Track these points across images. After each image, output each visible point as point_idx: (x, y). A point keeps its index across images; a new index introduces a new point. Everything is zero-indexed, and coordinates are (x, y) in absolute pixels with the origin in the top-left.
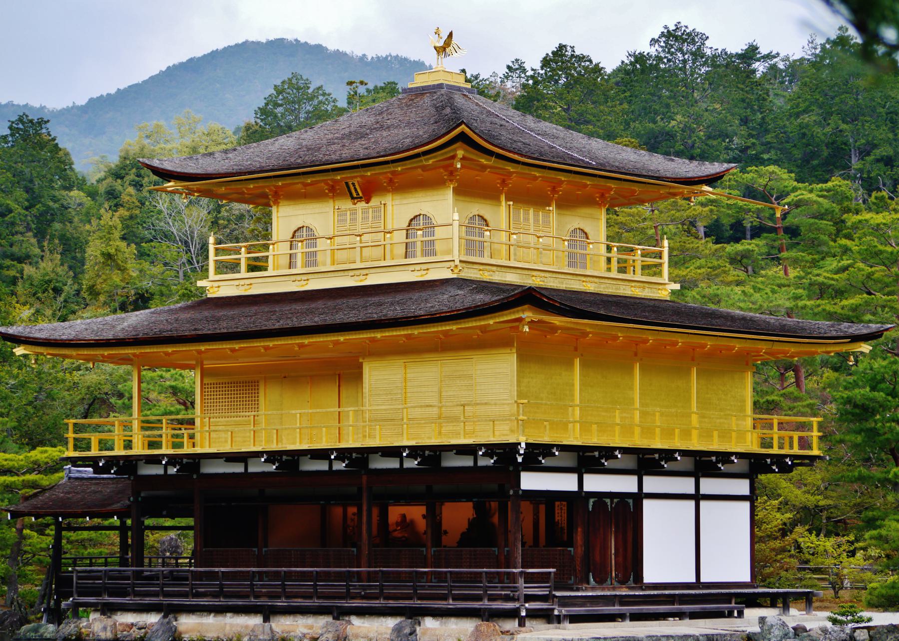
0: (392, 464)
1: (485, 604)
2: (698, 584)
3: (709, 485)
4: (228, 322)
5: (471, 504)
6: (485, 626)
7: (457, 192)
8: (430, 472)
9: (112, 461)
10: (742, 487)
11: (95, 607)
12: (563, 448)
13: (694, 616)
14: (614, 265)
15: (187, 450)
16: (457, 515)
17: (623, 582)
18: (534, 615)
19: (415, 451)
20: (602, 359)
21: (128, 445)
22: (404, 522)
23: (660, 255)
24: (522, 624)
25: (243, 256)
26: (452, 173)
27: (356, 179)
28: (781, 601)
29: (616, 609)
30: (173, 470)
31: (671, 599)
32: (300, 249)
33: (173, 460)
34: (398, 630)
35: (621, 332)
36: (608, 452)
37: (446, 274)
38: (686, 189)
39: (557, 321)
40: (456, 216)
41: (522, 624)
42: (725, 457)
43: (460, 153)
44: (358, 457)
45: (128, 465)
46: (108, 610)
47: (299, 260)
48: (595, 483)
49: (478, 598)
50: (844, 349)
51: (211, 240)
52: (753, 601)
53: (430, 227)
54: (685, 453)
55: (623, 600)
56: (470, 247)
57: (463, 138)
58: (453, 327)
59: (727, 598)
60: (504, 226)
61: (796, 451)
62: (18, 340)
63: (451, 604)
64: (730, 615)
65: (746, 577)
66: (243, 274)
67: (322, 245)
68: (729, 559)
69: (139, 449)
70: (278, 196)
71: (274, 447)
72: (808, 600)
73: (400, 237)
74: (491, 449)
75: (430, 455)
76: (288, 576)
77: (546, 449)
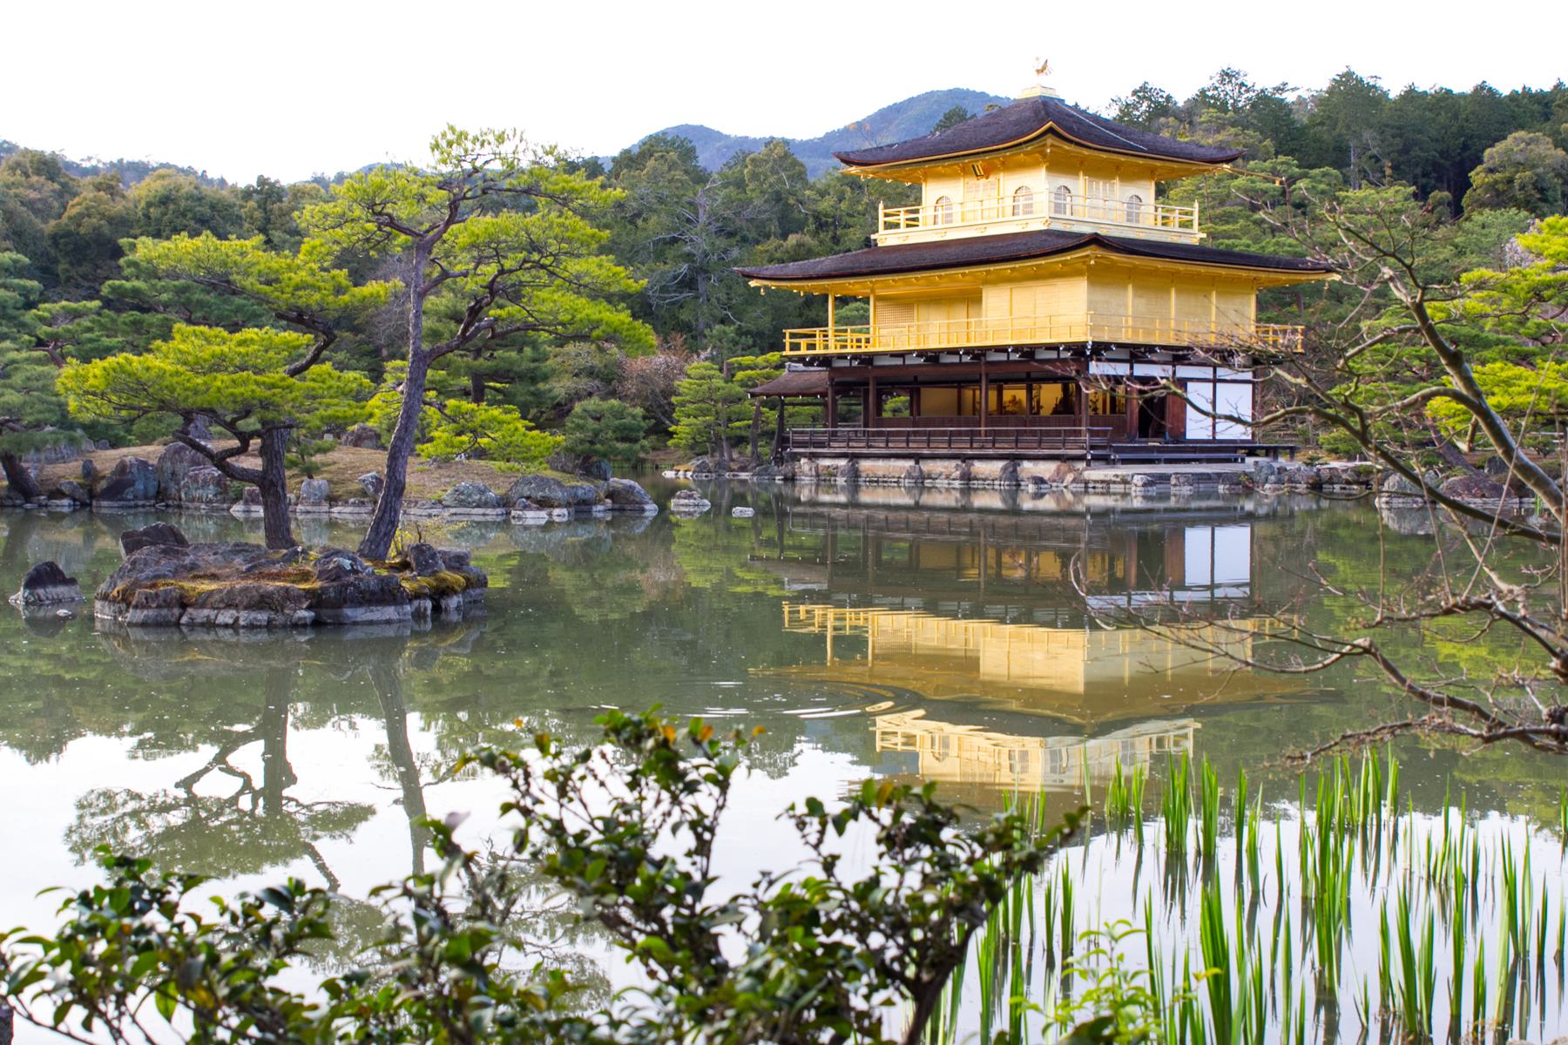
0: (1002, 357)
2: (1214, 440)
3: (1222, 372)
4: (891, 261)
5: (1059, 386)
6: (1064, 467)
7: (1049, 169)
8: (1027, 364)
9: (814, 358)
11: (803, 455)
12: (1119, 345)
13: (1209, 461)
14: (1160, 221)
15: (863, 350)
16: (1050, 395)
18: (1096, 458)
19: (1017, 348)
20: (1148, 284)
21: (826, 347)
22: (1014, 401)
23: (1191, 214)
24: (1088, 465)
26: (1044, 155)
27: (979, 165)
28: (1272, 452)
29: (1155, 455)
30: (855, 363)
31: (1195, 450)
32: (939, 213)
33: (855, 356)
34: (1004, 469)
35: (1159, 264)
36: (1151, 348)
37: (1037, 226)
38: (1210, 167)
39: (1115, 257)
44: (978, 353)
45: (825, 361)
46: (813, 457)
47: (939, 220)
48: (1141, 370)
50: (1320, 277)
51: (881, 206)
52: (1252, 452)
53: (1029, 196)
55: (1159, 450)
56: (1059, 208)
58: (1042, 262)
59: (1235, 450)
60: (1081, 192)
62: (752, 277)
64: (1236, 460)
66: (903, 228)
67: (956, 210)
69: (832, 351)
70: (926, 176)
71: (922, 347)
72: (1292, 451)
73: (1009, 202)
74: (1069, 347)
75: (1028, 352)
76: (930, 434)
77: (1106, 346)
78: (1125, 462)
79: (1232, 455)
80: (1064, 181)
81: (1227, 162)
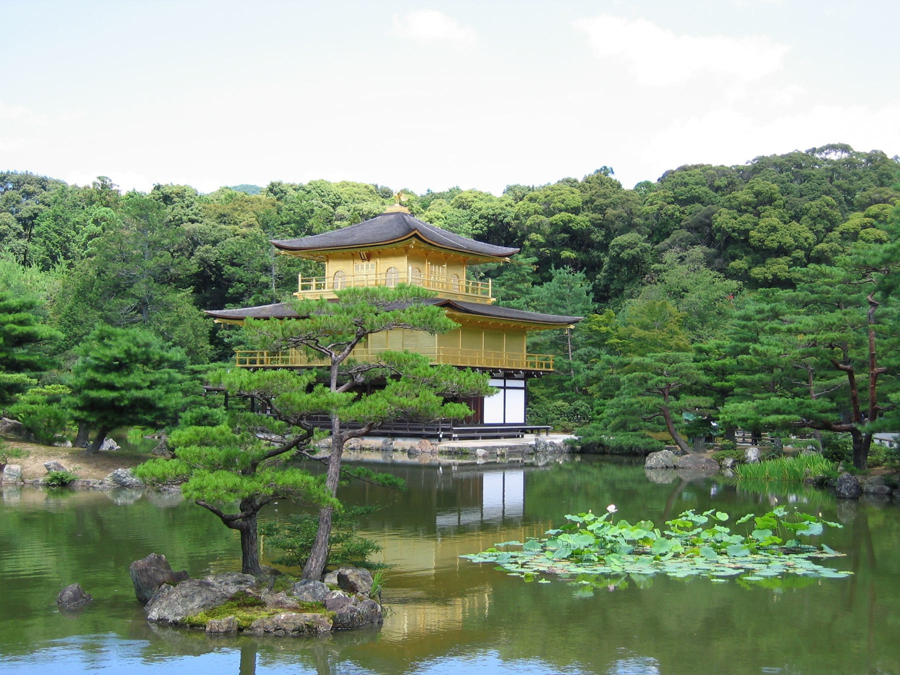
1: (424, 432)
2: (504, 424)
3: (510, 383)
10: (521, 384)
13: (506, 437)
17: (476, 424)
18: (444, 436)
24: (440, 441)
25: (314, 283)
27: (364, 252)
28: (538, 431)
29: (476, 434)
31: (496, 431)
34: (385, 443)
40: (410, 268)
41: (440, 441)
42: (517, 371)
43: (414, 242)
49: (421, 430)
52: (525, 431)
54: (502, 369)
57: (416, 236)
59: (517, 430)
61: (544, 369)
63: (409, 432)
64: (518, 437)
65: (521, 420)
68: (516, 413)
70: (328, 258)
73: (383, 277)
78: (461, 438)
79: (516, 434)
80: (416, 265)
81: (508, 256)
